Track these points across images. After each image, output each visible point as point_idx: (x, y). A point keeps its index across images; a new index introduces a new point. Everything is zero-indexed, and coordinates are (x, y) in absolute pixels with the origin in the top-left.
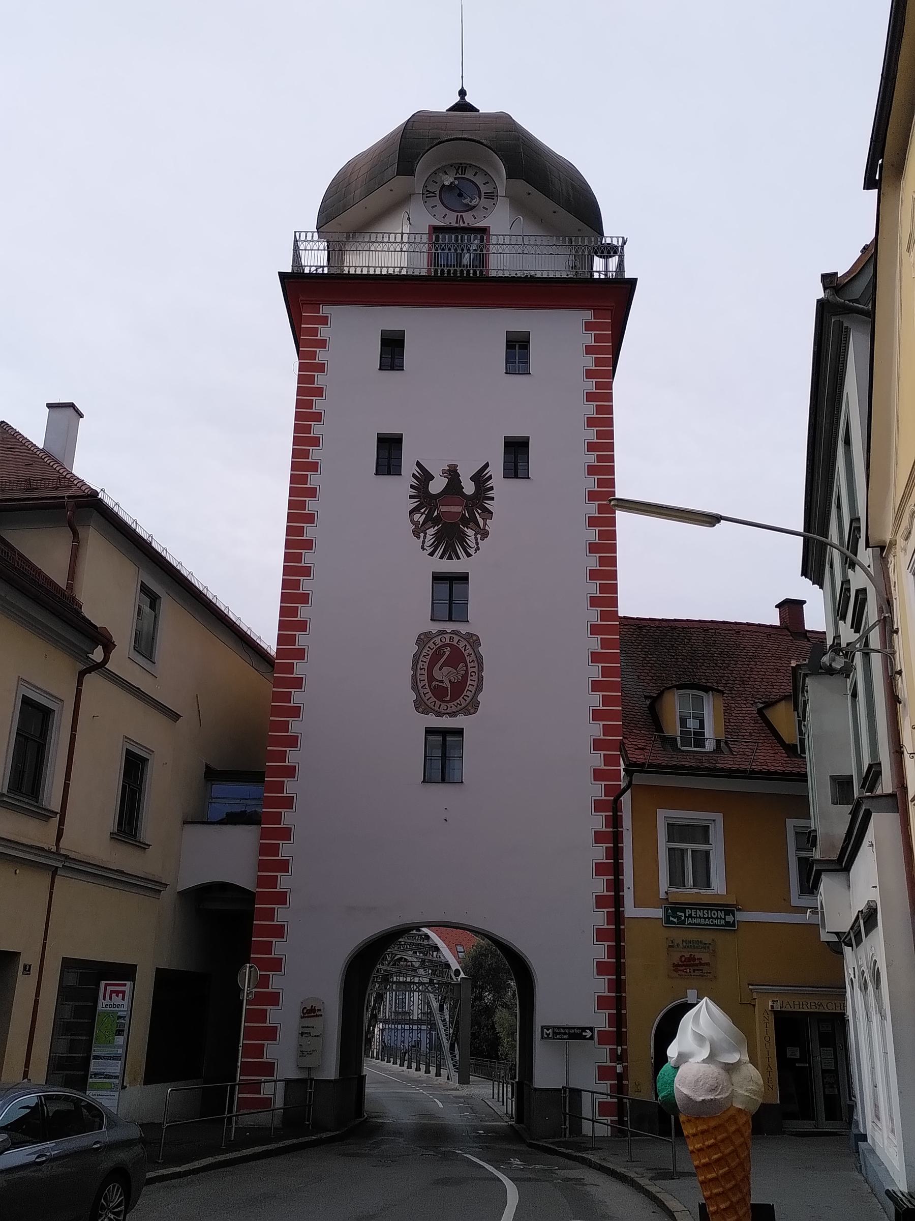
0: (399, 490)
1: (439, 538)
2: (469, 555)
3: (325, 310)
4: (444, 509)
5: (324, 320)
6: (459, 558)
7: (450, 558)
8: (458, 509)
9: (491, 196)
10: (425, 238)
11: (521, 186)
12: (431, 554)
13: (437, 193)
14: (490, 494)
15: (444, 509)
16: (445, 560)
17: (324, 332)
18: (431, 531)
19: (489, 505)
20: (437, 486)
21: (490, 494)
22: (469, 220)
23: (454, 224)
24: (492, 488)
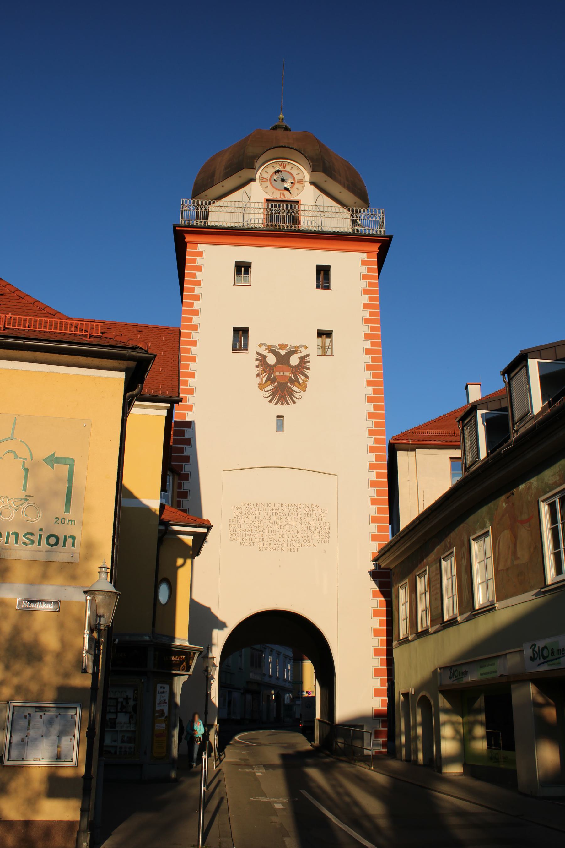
0: (248, 360)
1: (274, 393)
2: (294, 402)
3: (201, 247)
4: (277, 373)
5: (200, 254)
6: (288, 404)
7: (282, 404)
8: (288, 374)
9: (301, 182)
10: (260, 206)
11: (321, 177)
12: (270, 401)
13: (269, 179)
14: (308, 365)
15: (277, 373)
16: (279, 405)
17: (200, 261)
18: (270, 387)
19: (306, 372)
20: (271, 360)
21: (308, 365)
22: (288, 196)
23: (279, 198)
24: (309, 362)
